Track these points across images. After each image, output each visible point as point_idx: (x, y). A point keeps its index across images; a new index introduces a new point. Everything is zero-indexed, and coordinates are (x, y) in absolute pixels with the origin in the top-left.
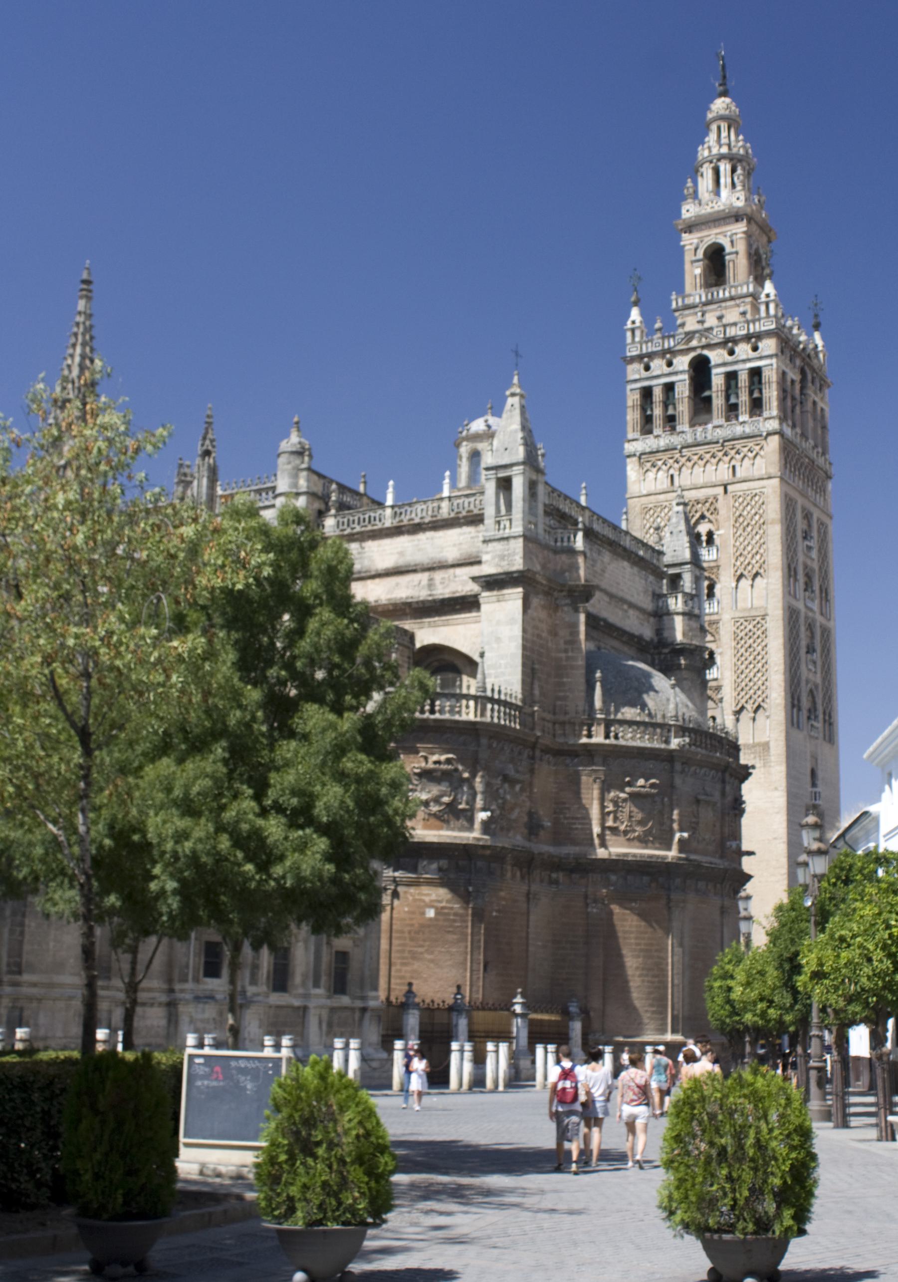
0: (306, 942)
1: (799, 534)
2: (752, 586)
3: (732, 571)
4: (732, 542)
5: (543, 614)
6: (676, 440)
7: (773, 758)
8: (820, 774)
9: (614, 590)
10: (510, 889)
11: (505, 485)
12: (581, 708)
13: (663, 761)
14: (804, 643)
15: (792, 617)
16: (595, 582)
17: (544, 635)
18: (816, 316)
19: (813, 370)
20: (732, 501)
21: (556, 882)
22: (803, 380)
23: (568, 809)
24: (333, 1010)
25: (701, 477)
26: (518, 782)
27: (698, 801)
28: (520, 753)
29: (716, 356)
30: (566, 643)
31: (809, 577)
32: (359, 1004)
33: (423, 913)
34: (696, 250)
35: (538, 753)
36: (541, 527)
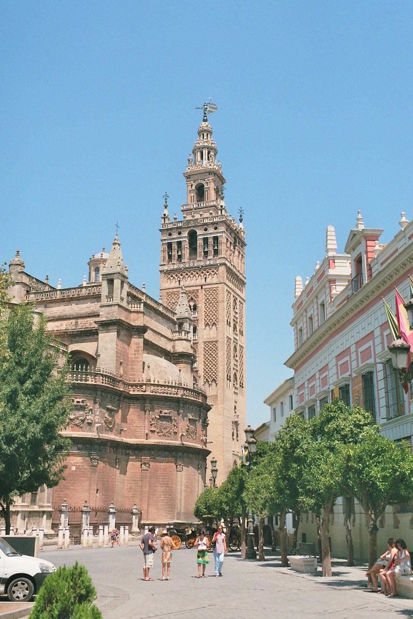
1: (232, 306)
3: (204, 322)
4: (204, 309)
6: (182, 266)
7: (219, 402)
11: (111, 282)
16: (148, 325)
18: (241, 216)
19: (239, 238)
20: (204, 292)
22: (235, 243)
25: (192, 281)
28: (114, 399)
30: (135, 351)
31: (234, 325)
34: (192, 185)
35: (122, 399)
36: (125, 300)
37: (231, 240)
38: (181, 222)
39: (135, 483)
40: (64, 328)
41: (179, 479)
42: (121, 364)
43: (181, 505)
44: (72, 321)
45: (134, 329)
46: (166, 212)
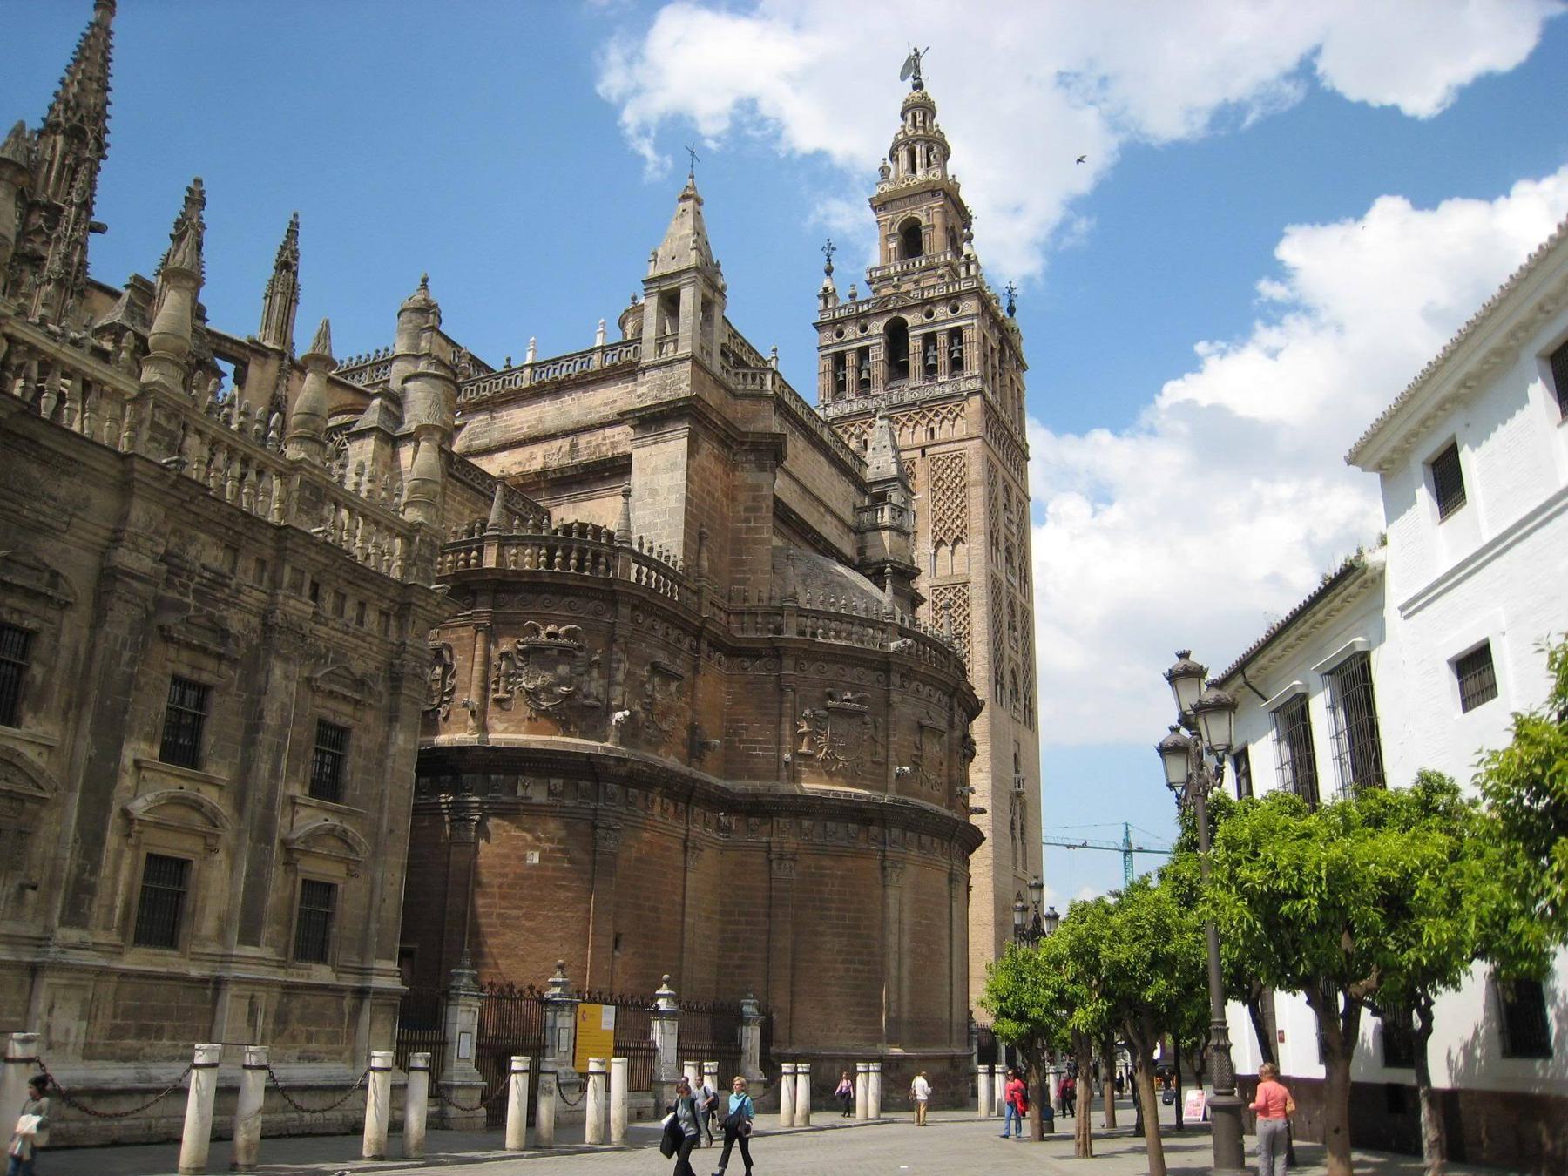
0: (233, 855)
2: (952, 552)
5: (718, 469)
8: (1022, 760)
9: (809, 485)
10: (657, 830)
11: (670, 303)
12: (765, 595)
13: (875, 669)
14: (1006, 619)
15: (995, 586)
17: (718, 494)
18: (1011, 301)
19: (1011, 348)
21: (728, 829)
22: (1002, 351)
23: (746, 729)
24: (290, 989)
26: (679, 678)
27: (921, 727)
29: (912, 319)
30: (746, 510)
31: (1007, 550)
32: (350, 981)
33: (524, 858)
35: (704, 646)
37: (993, 342)
38: (868, 302)
39: (747, 923)
40: (537, 465)
41: (893, 913)
42: (701, 539)
43: (899, 998)
44: (560, 441)
45: (742, 443)
46: (827, 282)
